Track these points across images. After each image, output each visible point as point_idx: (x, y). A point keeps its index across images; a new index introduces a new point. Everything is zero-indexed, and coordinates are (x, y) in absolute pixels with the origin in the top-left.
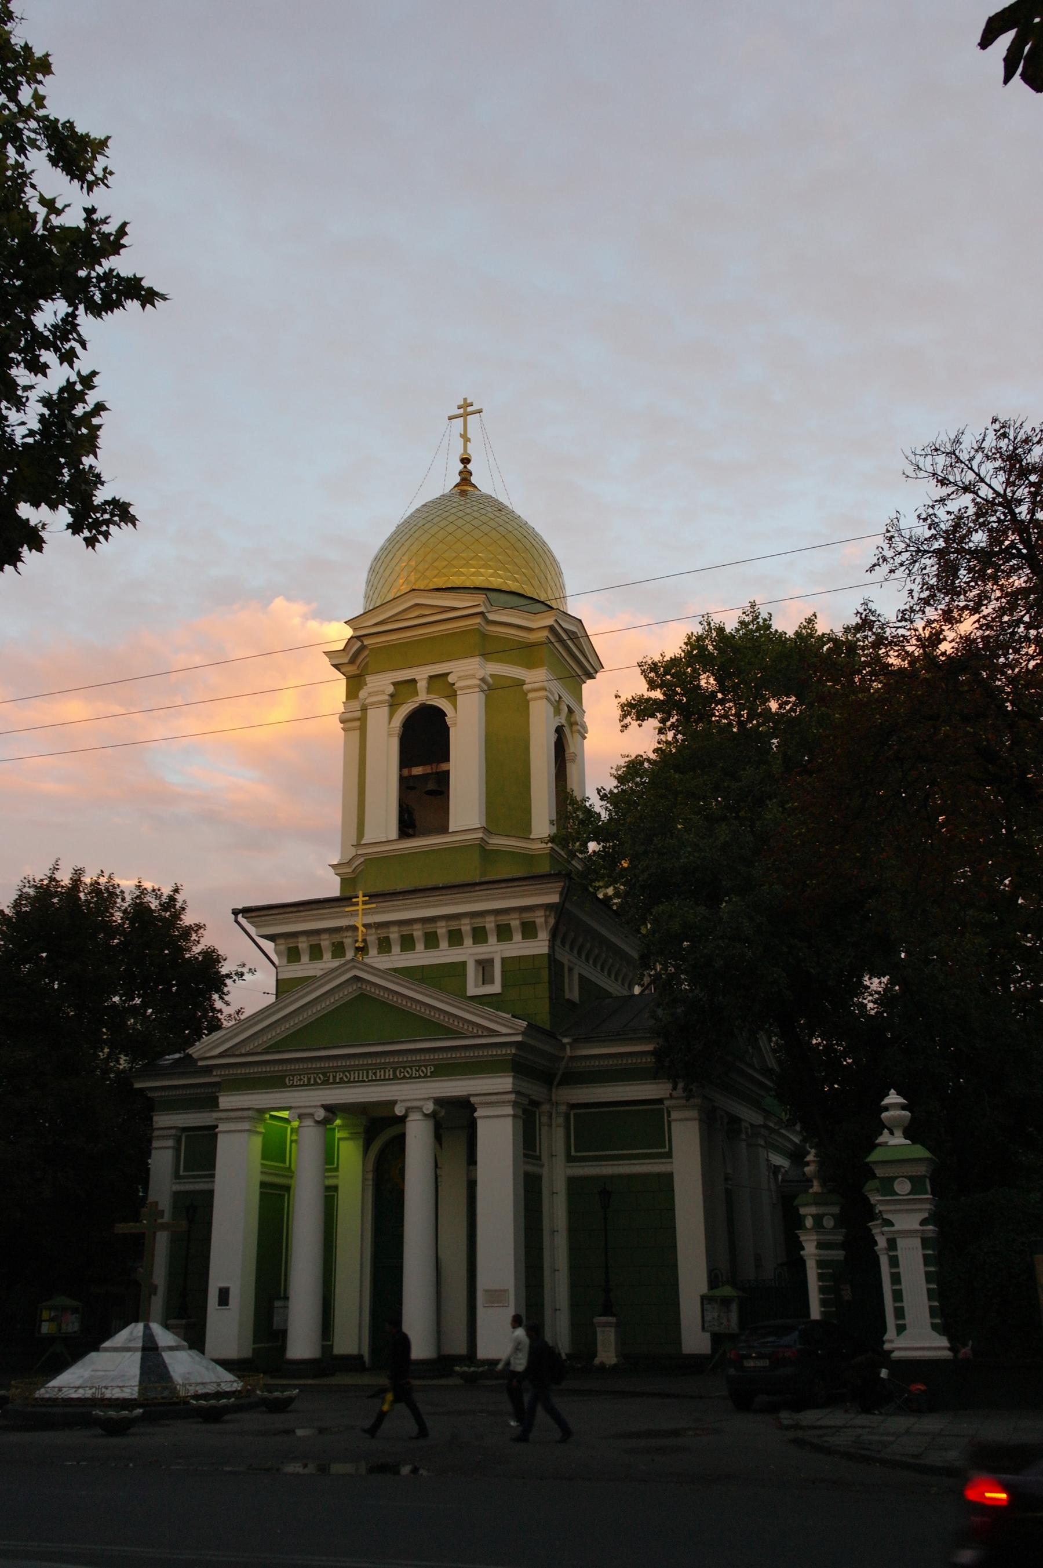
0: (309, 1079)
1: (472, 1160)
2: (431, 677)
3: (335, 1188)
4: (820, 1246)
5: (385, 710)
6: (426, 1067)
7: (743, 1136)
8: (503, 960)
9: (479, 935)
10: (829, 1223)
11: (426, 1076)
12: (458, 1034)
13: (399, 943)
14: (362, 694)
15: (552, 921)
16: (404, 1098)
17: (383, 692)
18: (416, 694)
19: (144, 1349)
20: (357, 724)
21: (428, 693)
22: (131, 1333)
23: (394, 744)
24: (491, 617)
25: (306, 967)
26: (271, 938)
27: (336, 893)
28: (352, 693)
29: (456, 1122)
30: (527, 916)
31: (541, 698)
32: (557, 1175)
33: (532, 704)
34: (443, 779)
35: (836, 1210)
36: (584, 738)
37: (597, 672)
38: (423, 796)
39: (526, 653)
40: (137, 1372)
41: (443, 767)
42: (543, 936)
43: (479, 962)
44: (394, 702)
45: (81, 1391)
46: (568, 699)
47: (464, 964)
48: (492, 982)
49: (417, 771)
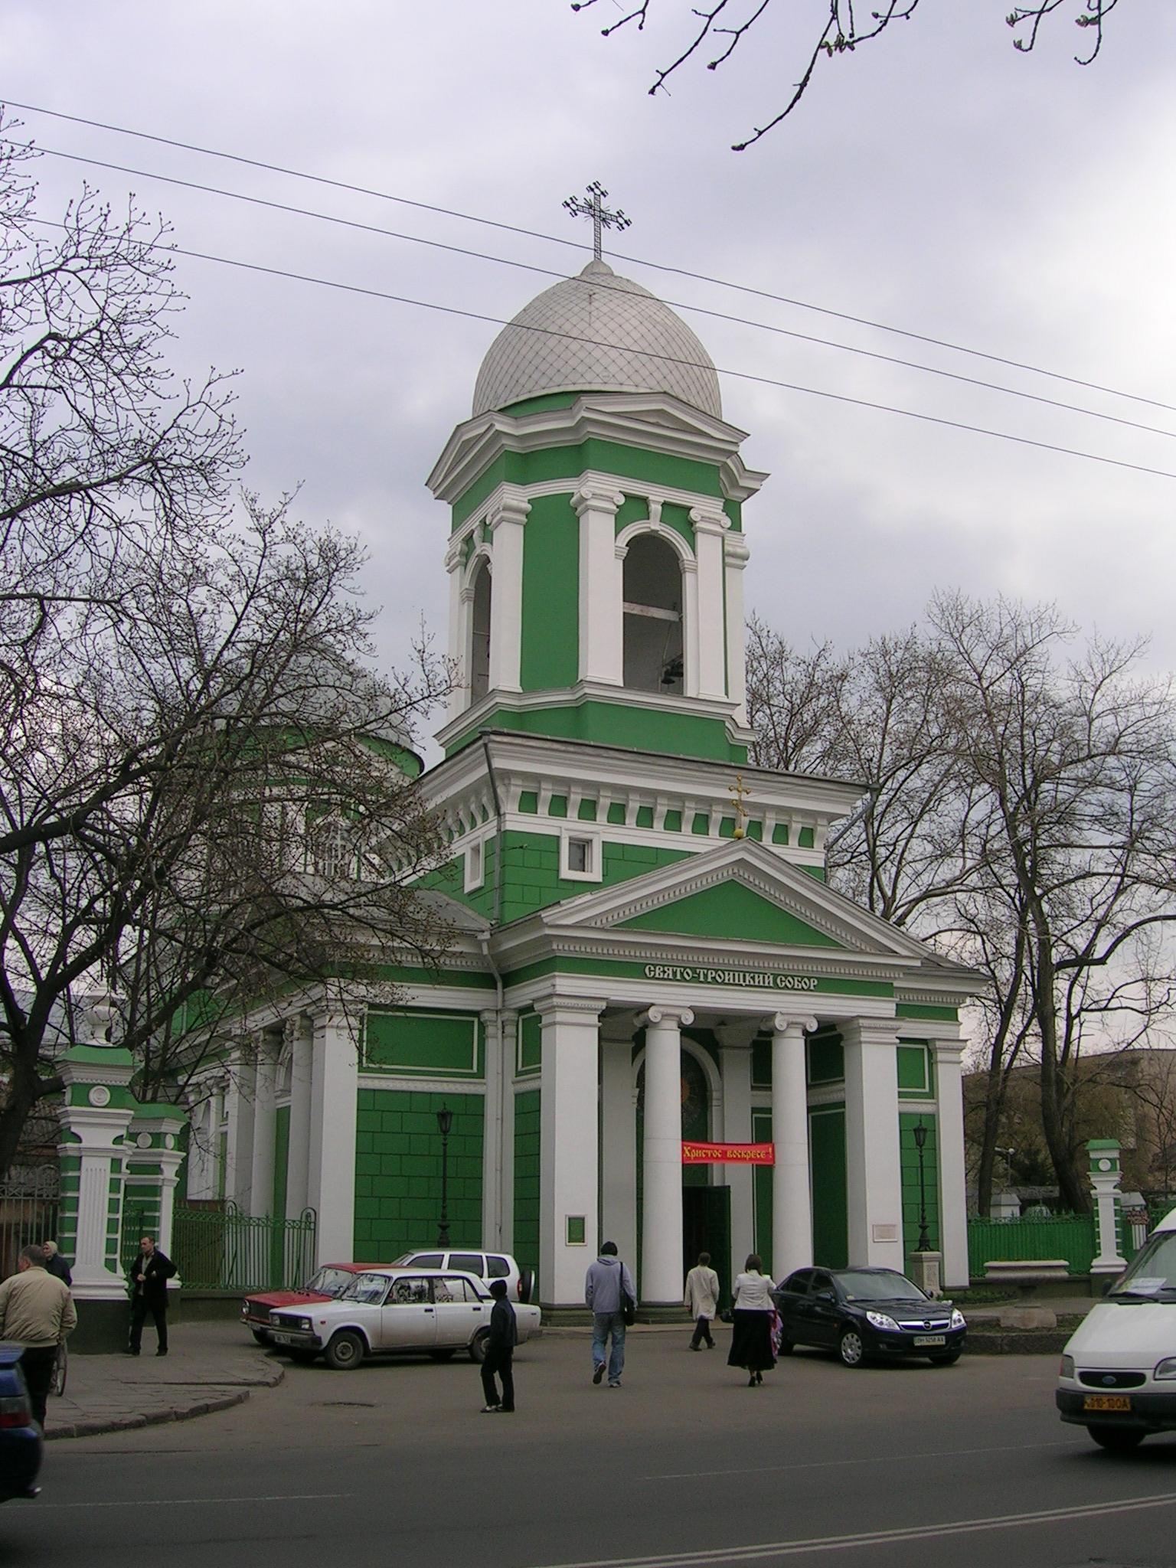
0: (675, 973)
2: (665, 504)
6: (809, 978)
11: (809, 989)
13: (656, 815)
16: (784, 1010)
17: (611, 499)
18: (647, 517)
23: (619, 565)
25: (543, 821)
44: (622, 519)
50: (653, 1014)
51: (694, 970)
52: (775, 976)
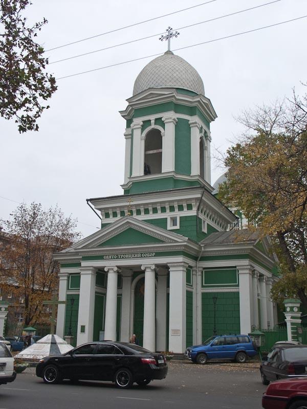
1: (168, 286)
3: (121, 295)
4: (292, 317)
5: (140, 130)
7: (265, 281)
8: (180, 217)
9: (172, 209)
10: (296, 310)
12: (163, 242)
13: (143, 211)
14: (132, 125)
15: (198, 204)
17: (139, 124)
19: (52, 343)
20: (130, 136)
21: (155, 124)
22: (48, 338)
23: (143, 142)
24: (177, 97)
26: (100, 209)
27: (122, 193)
28: (128, 126)
29: (163, 273)
30: (189, 203)
31: (195, 126)
32: (198, 291)
33: (192, 129)
34: (160, 155)
35: (299, 305)
36: (210, 142)
37: (215, 118)
38: (152, 163)
39: (192, 111)
40: (49, 351)
41: (160, 150)
42: (195, 209)
43: (171, 218)
45: (29, 356)
46: (205, 127)
47: (167, 218)
48: (176, 225)
49: (151, 152)
50: (106, 270)
51: (117, 255)
52: (141, 254)
